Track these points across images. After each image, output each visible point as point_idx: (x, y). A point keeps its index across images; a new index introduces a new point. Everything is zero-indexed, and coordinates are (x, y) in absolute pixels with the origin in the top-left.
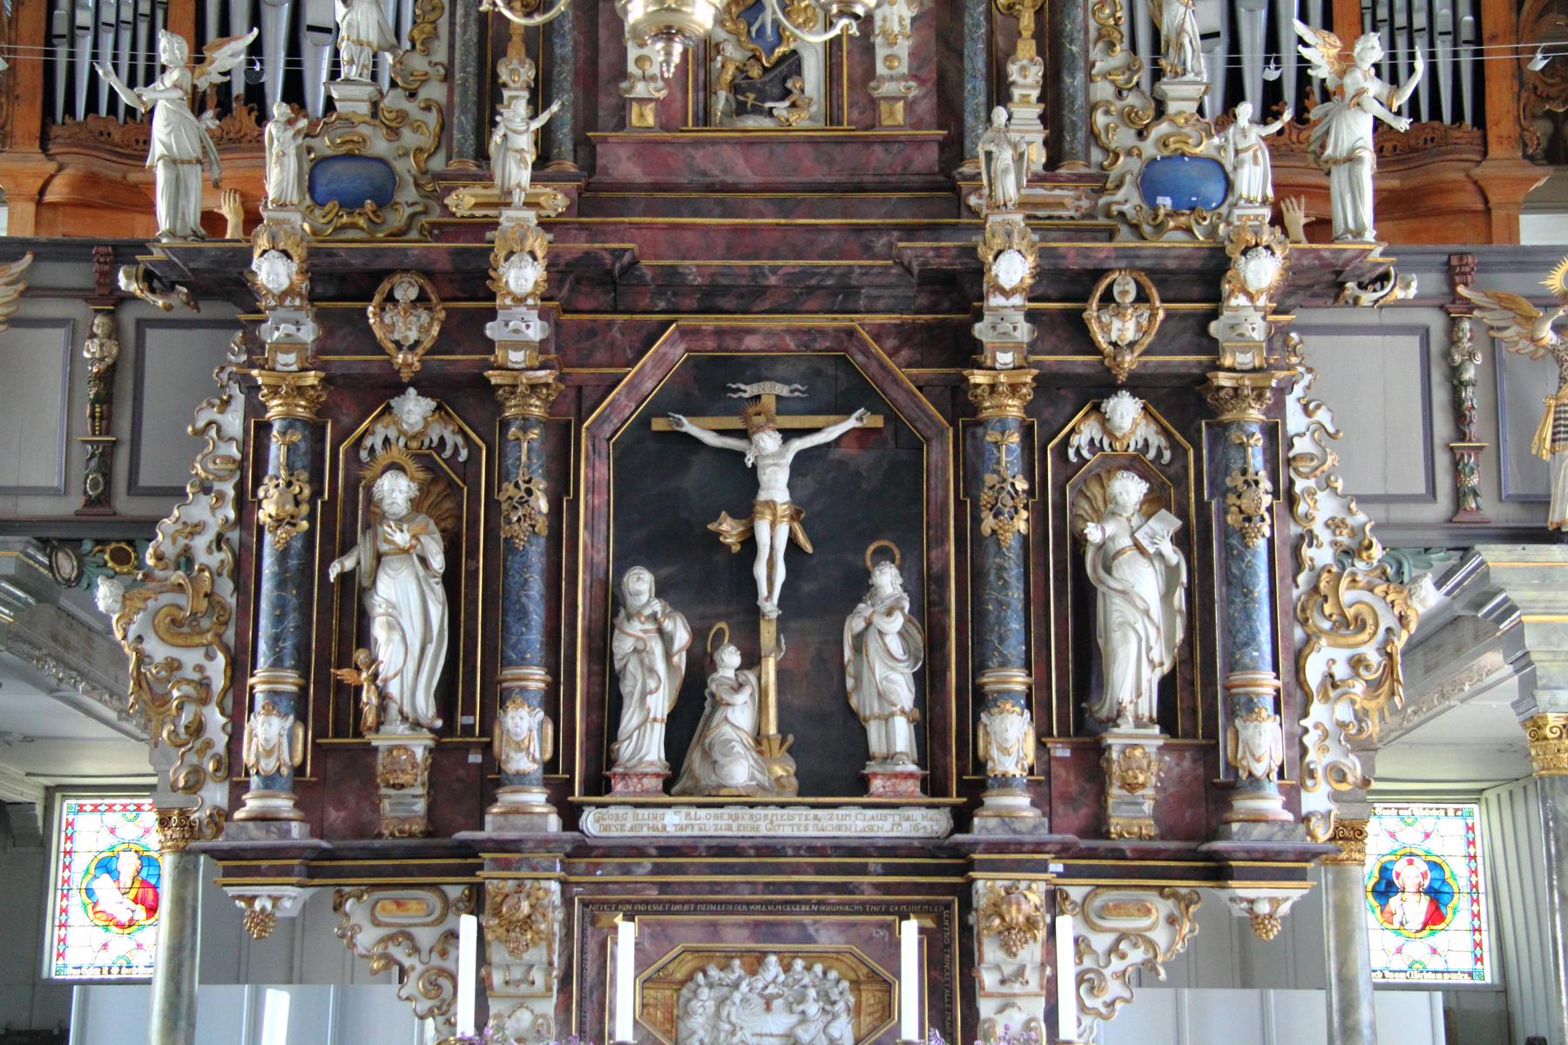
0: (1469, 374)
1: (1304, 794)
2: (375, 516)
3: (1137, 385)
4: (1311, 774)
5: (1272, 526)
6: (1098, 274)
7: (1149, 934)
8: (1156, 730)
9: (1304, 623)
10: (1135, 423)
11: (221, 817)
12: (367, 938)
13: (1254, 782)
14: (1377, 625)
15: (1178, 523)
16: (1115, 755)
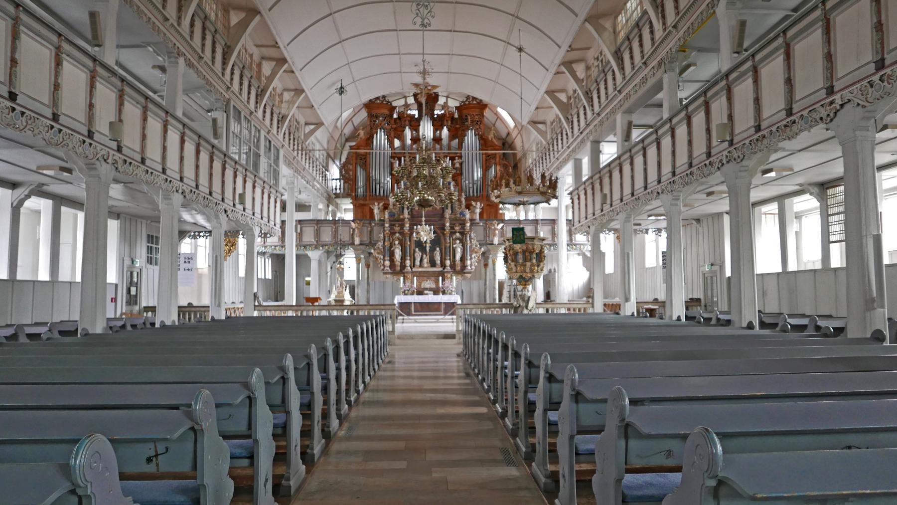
2: (395, 244)
11: (383, 270)
12: (395, 279)
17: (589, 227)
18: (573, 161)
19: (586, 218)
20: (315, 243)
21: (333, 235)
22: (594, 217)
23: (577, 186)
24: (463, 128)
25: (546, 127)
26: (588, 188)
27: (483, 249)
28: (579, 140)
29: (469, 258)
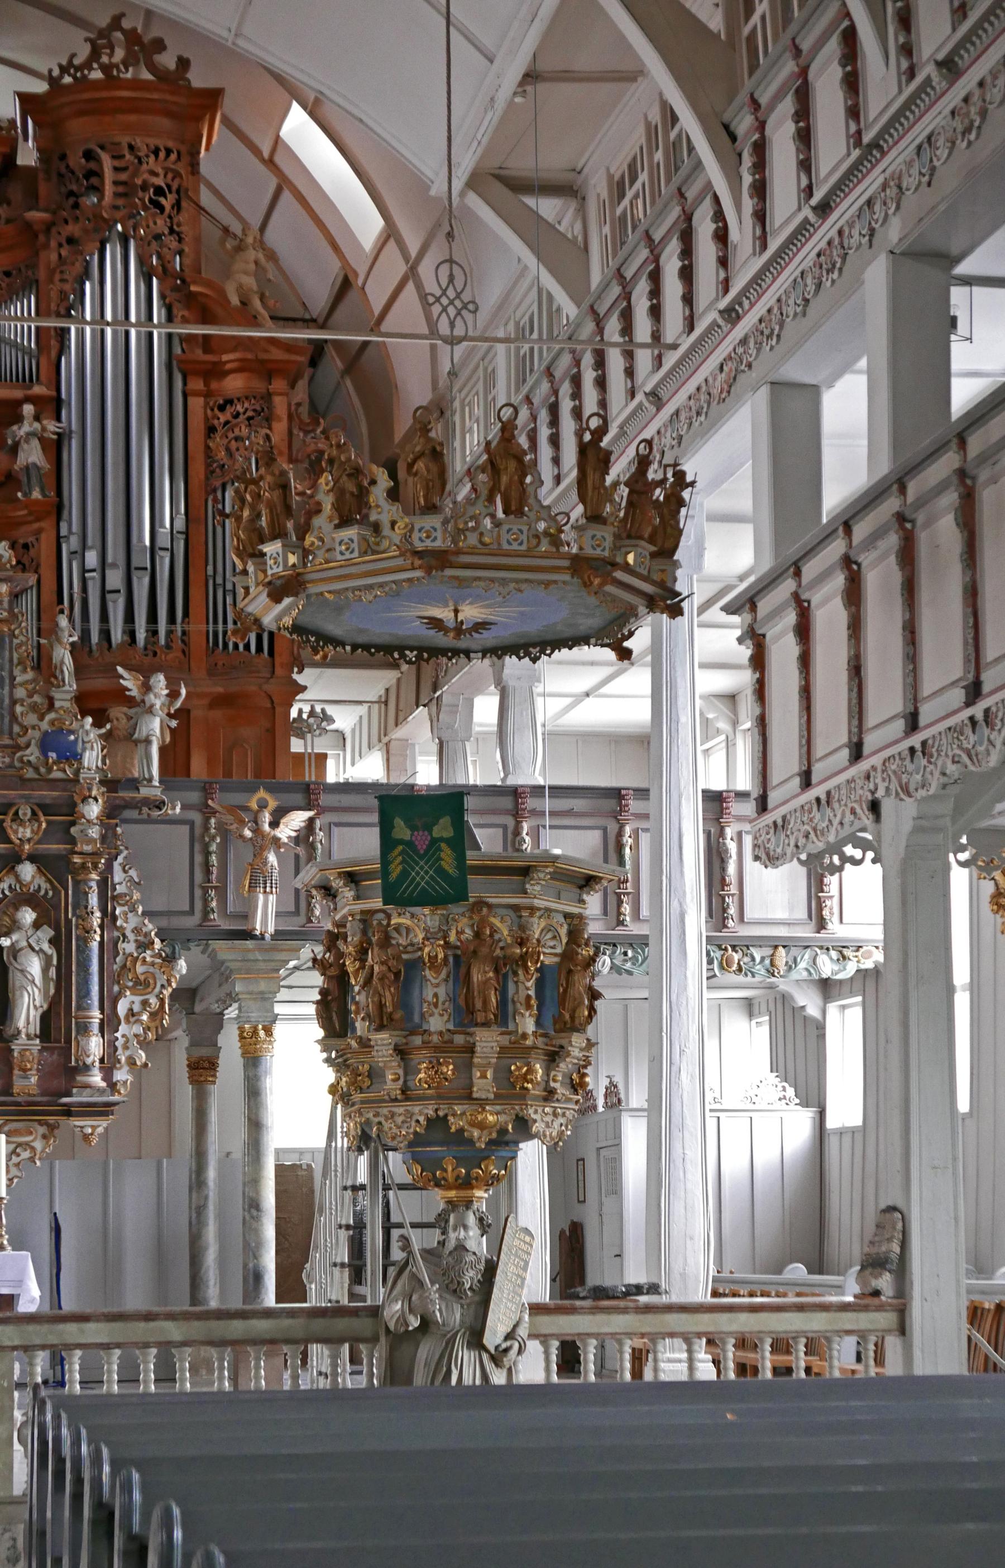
0: (213, 847)
1: (115, 1072)
3: (32, 858)
4: (119, 1061)
5: (102, 936)
6: (10, 805)
7: (32, 1144)
8: (38, 1041)
9: (119, 983)
10: (33, 877)
13: (87, 1068)
14: (155, 984)
15: (52, 933)
16: (16, 1054)
17: (875, 807)
18: (764, 392)
19: (857, 753)
22: (915, 740)
23: (793, 551)
24: (72, 229)
25: (582, 211)
26: (866, 559)
27: (182, 965)
28: (806, 256)
29: (96, 1015)
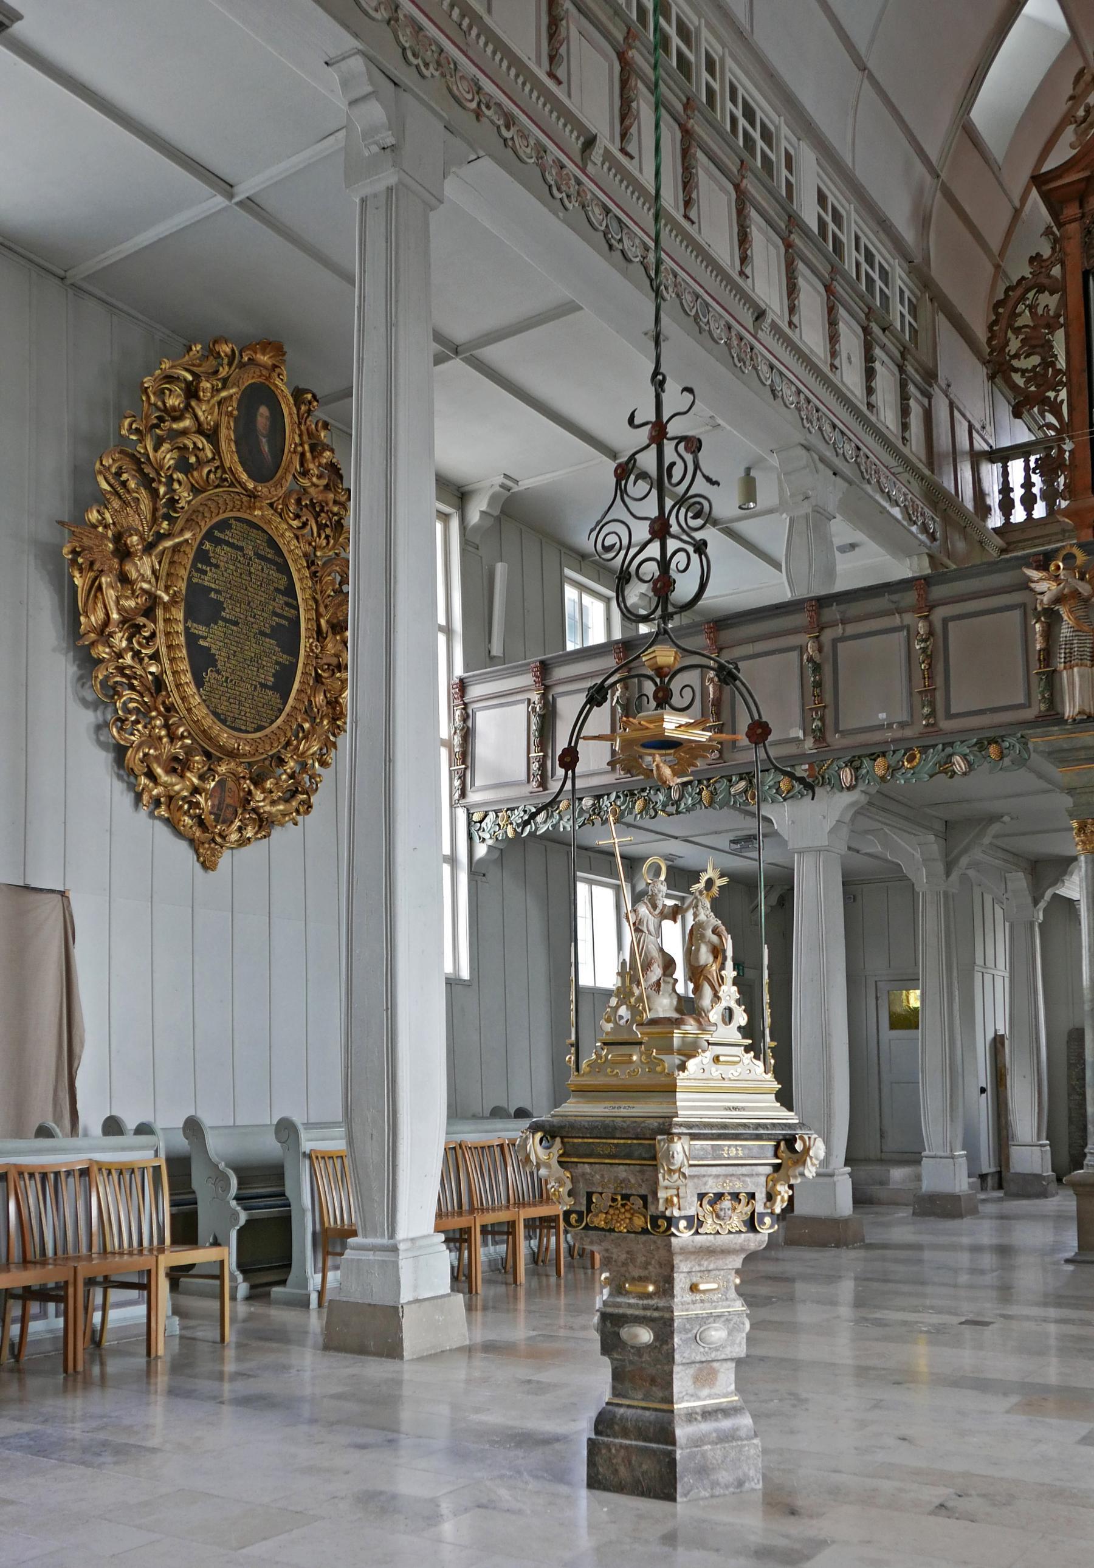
20: (809, 744)
21: (919, 685)
